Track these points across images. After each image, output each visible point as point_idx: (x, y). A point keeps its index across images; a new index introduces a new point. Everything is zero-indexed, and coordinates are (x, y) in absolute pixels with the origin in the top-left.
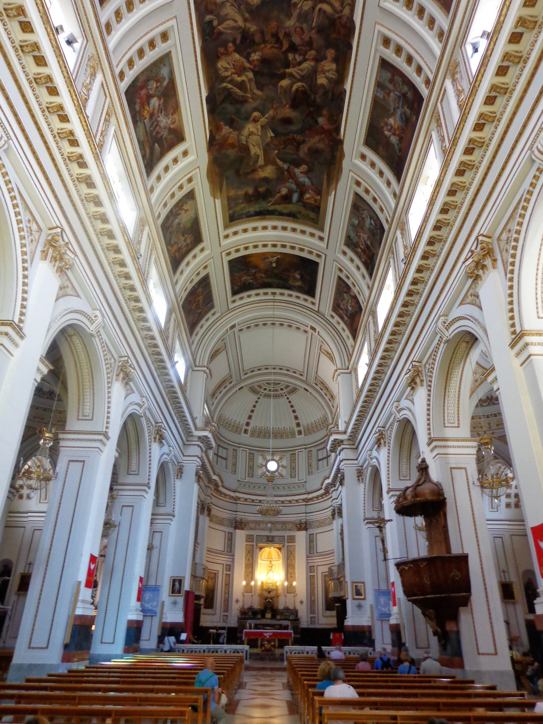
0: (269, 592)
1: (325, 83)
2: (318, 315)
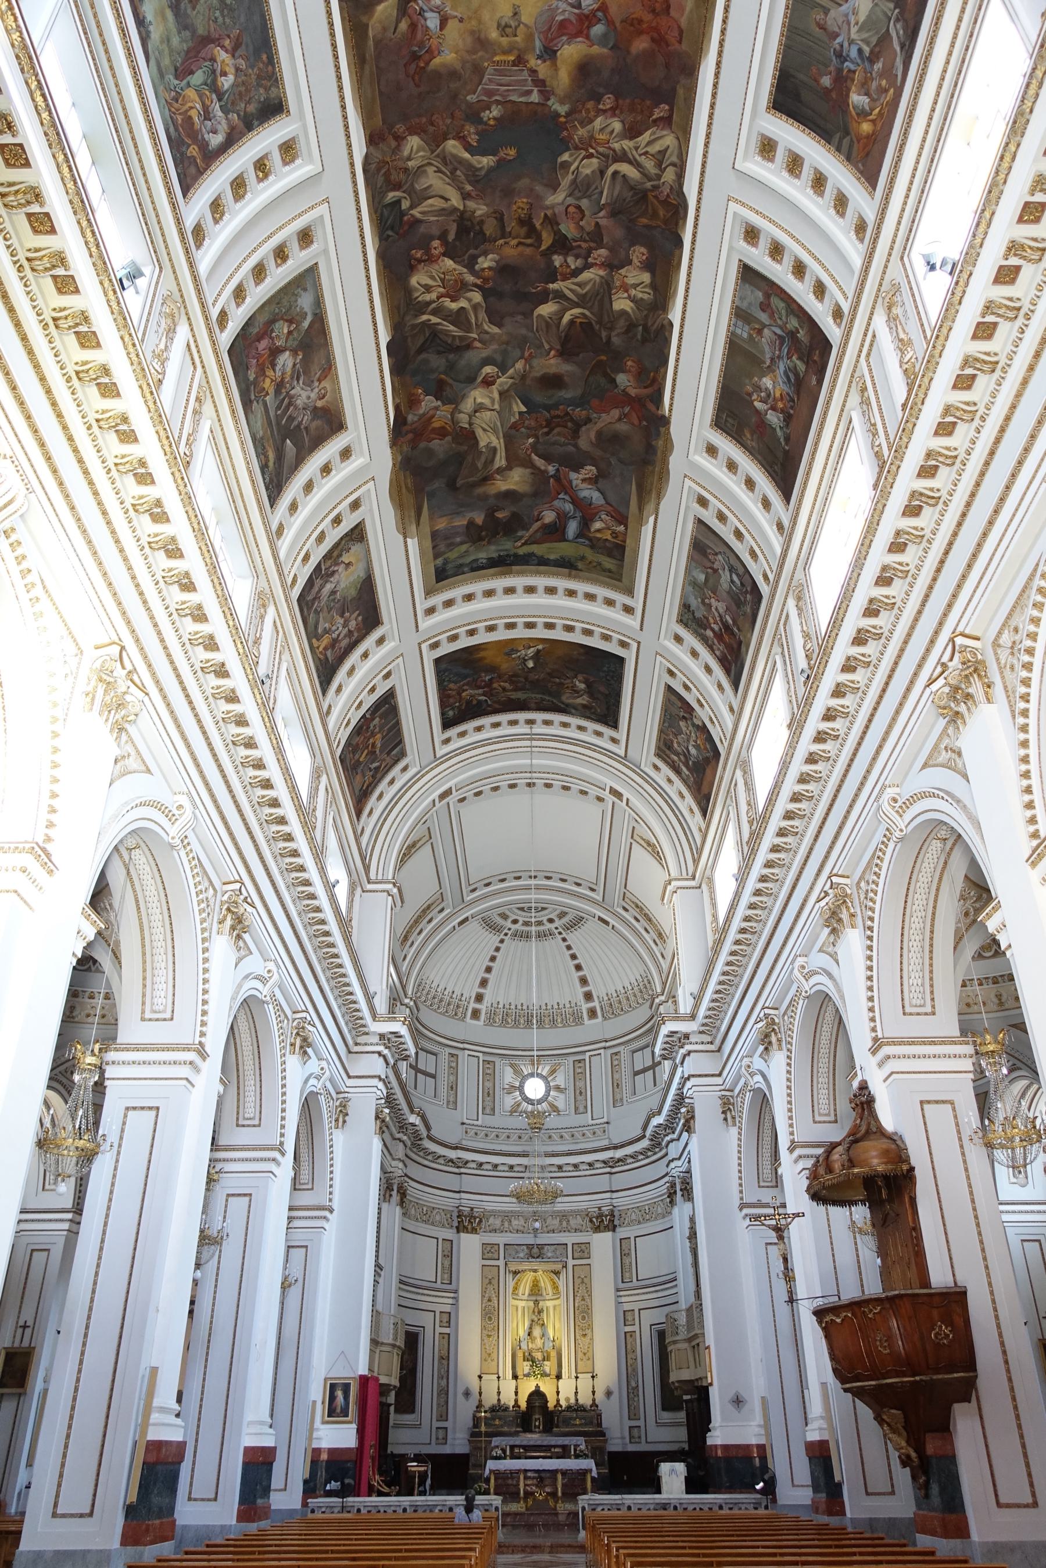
1: (628, 309)
2: (625, 765)
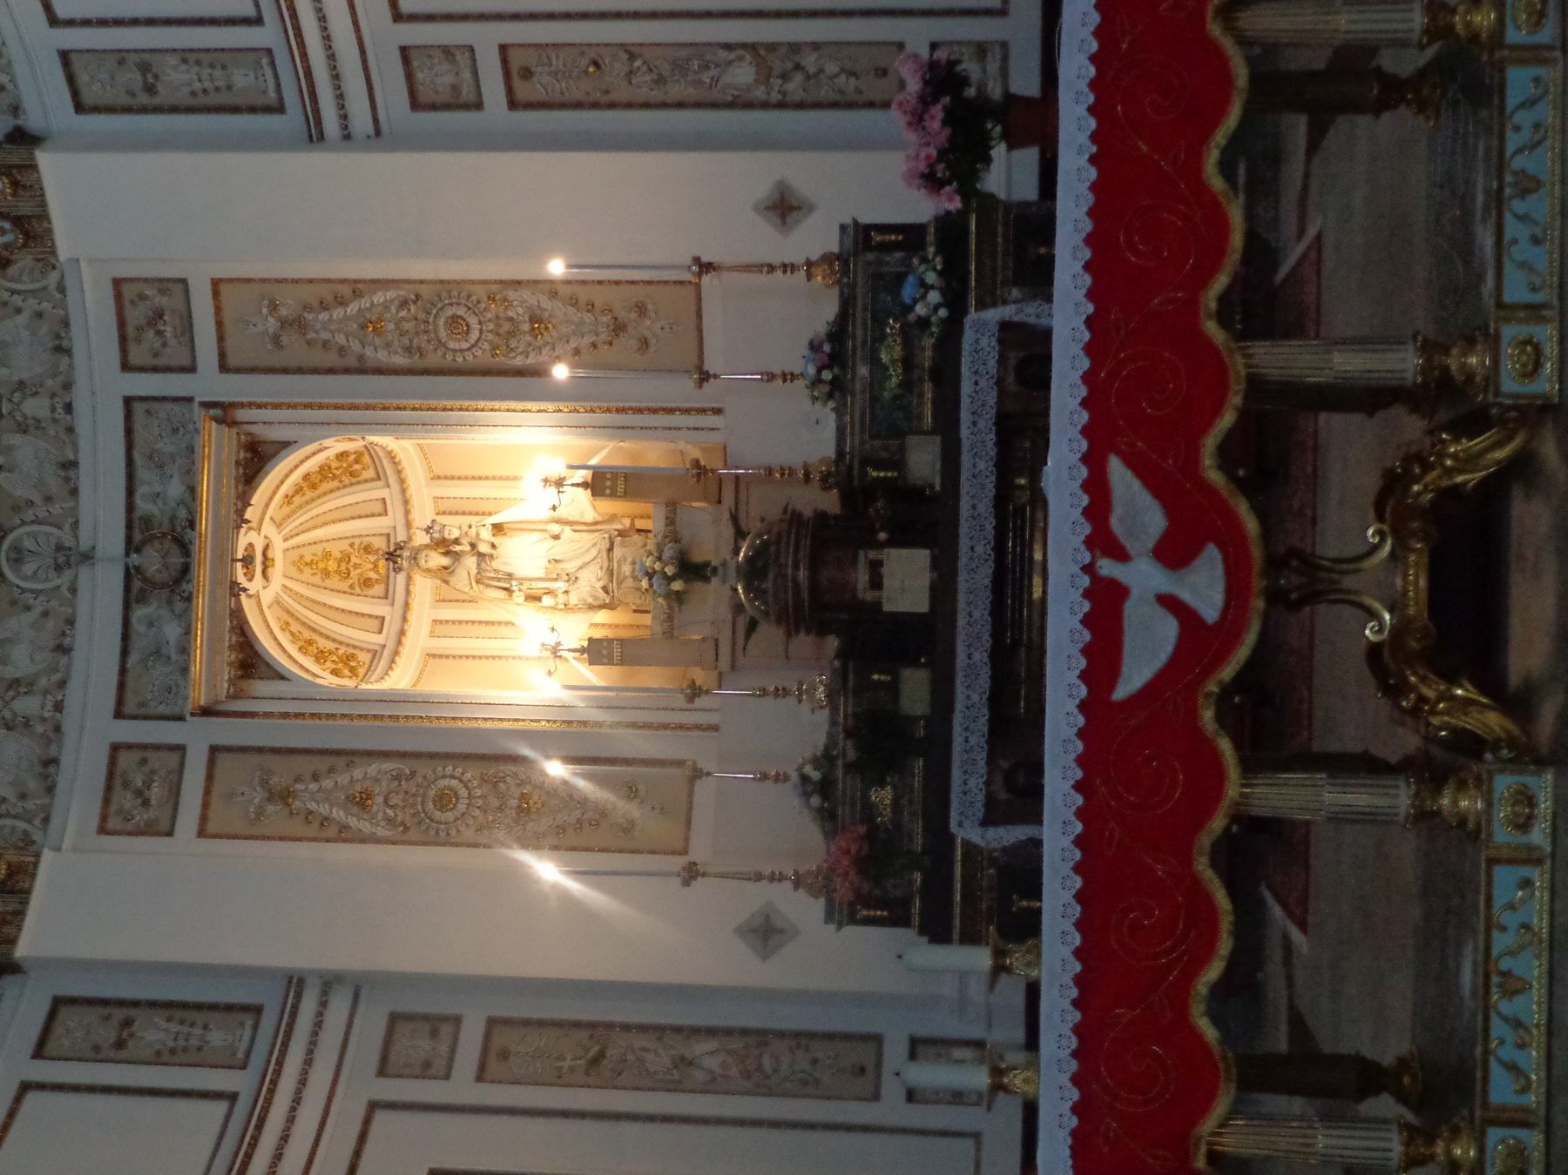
0: (692, 570)
